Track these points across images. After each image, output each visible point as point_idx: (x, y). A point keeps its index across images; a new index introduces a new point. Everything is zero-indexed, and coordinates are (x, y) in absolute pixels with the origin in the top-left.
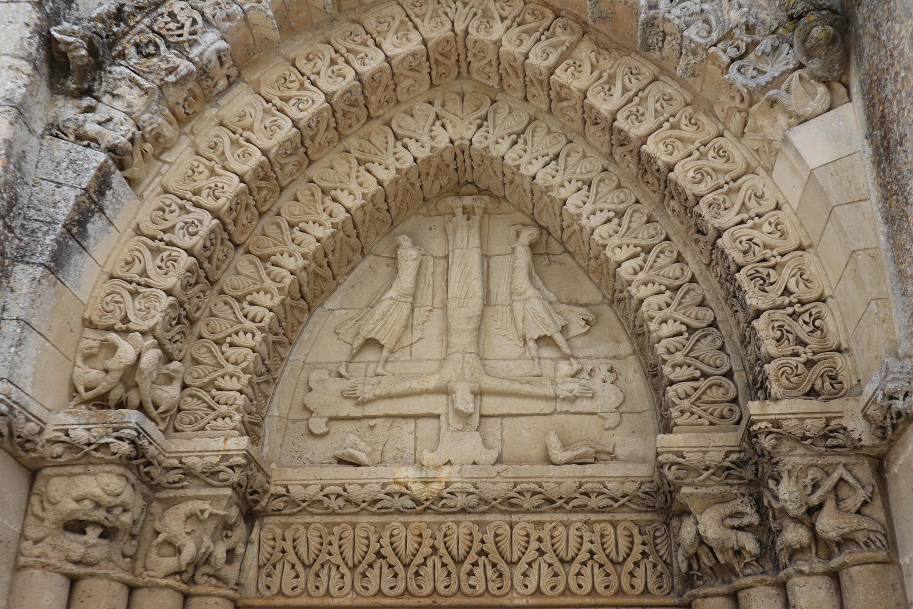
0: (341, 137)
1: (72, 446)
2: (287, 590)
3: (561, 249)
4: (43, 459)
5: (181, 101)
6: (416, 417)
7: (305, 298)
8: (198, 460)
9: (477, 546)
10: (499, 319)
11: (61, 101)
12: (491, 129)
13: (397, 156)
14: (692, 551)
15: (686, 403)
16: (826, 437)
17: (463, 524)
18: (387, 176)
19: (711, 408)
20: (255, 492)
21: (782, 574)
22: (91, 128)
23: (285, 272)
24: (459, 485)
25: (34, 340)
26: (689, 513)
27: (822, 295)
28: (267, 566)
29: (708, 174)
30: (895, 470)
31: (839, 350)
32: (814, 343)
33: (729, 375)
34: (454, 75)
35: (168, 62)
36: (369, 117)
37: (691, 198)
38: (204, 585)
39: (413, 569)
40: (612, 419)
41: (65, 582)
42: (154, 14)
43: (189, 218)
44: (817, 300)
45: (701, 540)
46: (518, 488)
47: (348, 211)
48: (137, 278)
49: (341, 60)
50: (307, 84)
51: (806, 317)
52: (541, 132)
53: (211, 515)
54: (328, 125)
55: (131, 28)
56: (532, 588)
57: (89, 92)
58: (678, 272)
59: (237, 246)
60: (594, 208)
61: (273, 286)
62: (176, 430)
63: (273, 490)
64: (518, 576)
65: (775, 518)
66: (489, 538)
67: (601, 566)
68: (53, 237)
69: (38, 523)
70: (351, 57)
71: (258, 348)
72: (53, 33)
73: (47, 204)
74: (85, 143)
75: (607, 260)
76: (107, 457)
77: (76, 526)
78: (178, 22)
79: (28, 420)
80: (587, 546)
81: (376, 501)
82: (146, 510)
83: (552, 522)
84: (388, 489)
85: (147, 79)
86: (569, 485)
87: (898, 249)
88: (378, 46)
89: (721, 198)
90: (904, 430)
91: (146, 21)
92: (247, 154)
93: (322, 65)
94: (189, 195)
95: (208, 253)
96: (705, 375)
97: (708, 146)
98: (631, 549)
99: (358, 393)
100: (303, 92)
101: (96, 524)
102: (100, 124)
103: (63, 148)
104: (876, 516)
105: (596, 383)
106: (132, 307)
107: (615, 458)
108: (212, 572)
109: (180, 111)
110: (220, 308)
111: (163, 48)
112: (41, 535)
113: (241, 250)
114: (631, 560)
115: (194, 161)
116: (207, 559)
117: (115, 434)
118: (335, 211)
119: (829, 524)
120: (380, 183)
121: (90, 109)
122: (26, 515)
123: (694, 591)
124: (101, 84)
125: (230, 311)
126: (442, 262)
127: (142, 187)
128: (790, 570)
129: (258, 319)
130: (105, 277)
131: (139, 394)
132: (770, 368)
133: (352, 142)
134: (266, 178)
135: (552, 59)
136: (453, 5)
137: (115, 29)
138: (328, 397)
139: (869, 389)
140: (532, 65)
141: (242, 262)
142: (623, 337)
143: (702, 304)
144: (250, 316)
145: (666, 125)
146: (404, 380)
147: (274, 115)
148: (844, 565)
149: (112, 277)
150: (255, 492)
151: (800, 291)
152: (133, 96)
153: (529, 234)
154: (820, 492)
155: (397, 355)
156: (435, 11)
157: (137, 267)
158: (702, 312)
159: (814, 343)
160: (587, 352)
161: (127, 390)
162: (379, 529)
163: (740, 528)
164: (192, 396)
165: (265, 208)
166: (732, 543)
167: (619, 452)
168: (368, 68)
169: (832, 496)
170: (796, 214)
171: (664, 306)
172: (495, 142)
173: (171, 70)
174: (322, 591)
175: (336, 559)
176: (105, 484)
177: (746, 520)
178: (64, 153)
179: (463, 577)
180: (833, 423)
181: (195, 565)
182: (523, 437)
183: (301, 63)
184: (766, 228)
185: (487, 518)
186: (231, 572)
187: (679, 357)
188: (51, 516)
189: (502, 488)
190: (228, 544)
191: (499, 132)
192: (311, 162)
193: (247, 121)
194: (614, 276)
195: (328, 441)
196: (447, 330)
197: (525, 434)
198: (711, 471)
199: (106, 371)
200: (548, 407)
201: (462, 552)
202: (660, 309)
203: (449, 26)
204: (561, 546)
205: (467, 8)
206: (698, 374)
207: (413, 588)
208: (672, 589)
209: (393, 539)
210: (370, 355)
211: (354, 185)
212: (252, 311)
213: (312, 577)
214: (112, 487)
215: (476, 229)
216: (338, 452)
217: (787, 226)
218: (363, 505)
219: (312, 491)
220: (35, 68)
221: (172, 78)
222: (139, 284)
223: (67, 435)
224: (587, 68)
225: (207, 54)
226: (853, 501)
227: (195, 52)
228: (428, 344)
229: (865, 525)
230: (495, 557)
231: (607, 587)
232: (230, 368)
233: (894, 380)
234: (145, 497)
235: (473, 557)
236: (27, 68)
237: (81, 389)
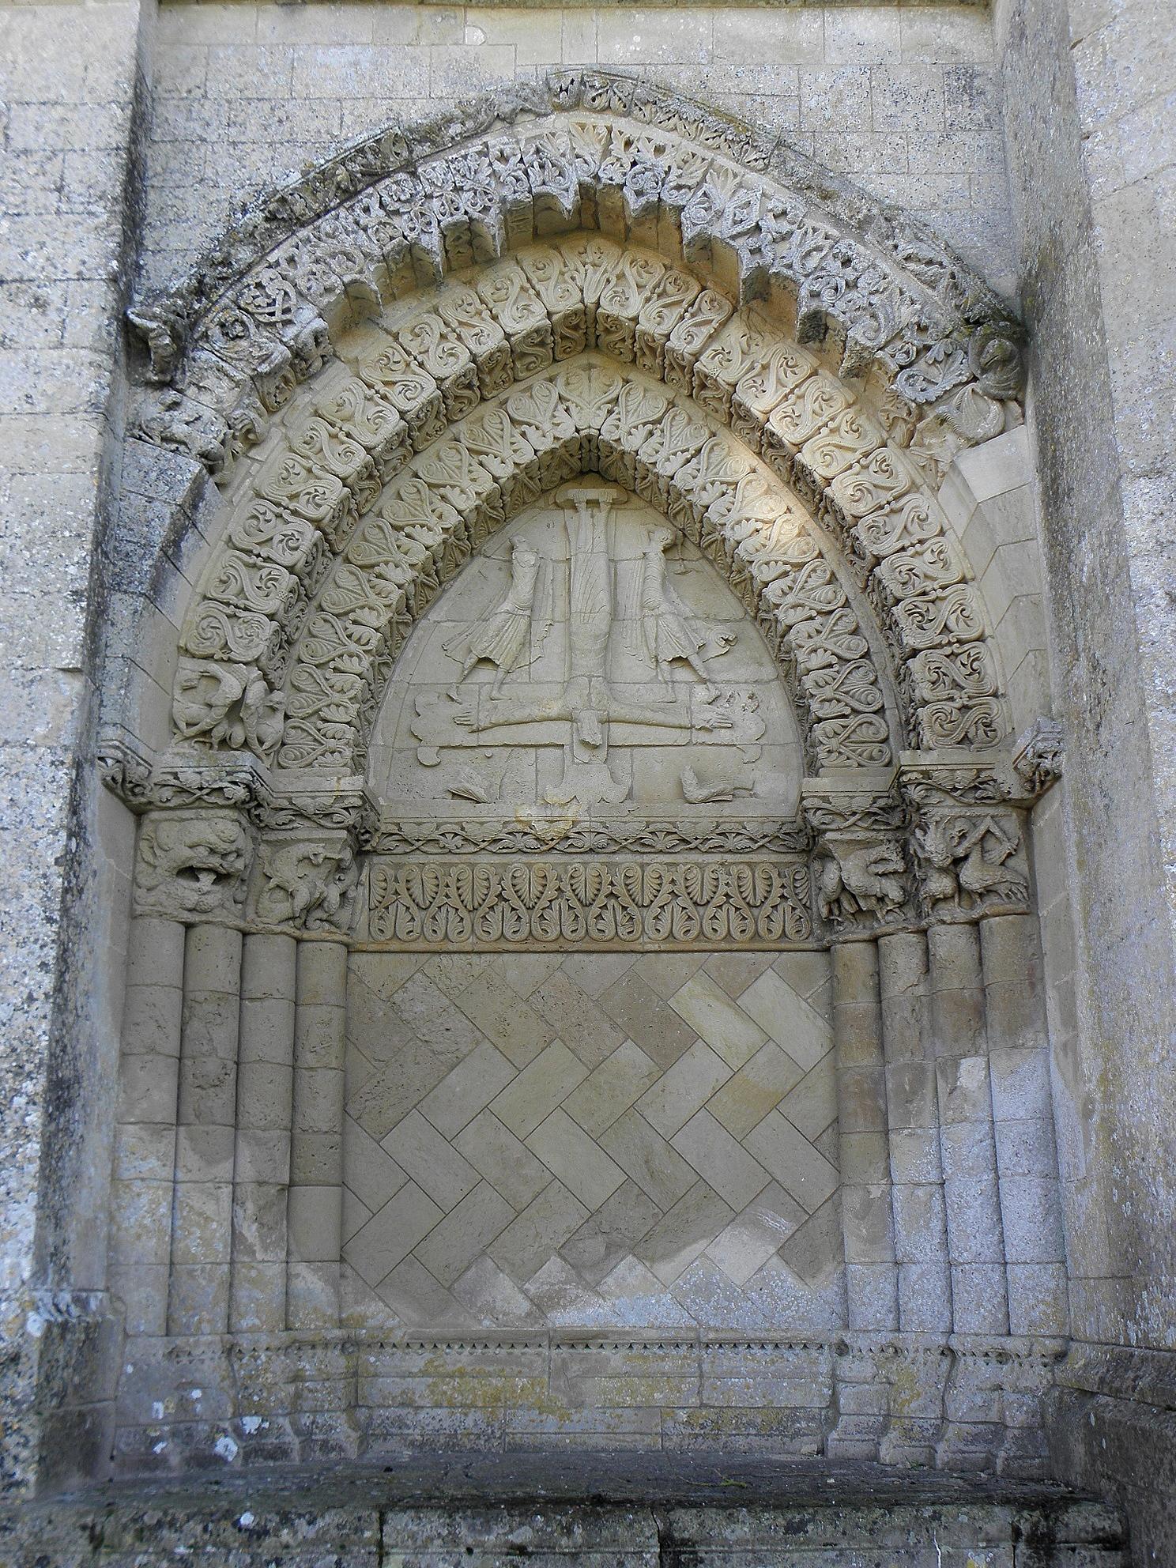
0: (450, 422)
2: (402, 935)
3: (699, 555)
4: (150, 803)
5: (273, 390)
7: (409, 613)
8: (309, 800)
9: (606, 889)
11: (141, 394)
12: (622, 416)
13: (515, 447)
14: (834, 897)
15: (834, 743)
16: (976, 788)
17: (591, 866)
18: (505, 472)
19: (860, 748)
20: (367, 832)
21: (923, 923)
22: (179, 430)
23: (392, 587)
24: (587, 824)
25: (139, 678)
26: (833, 858)
27: (982, 634)
28: (380, 908)
29: (869, 491)
30: (1041, 823)
31: (995, 695)
32: (970, 687)
34: (580, 348)
35: (261, 349)
36: (483, 399)
37: (849, 519)
38: (317, 930)
39: (537, 913)
40: (752, 752)
41: (182, 929)
42: (239, 286)
44: (977, 640)
45: (843, 887)
46: (651, 829)
47: (460, 512)
48: (234, 600)
49: (452, 337)
50: (414, 365)
51: (964, 658)
52: (682, 419)
53: (326, 858)
54: (438, 413)
55: (214, 304)
56: (664, 932)
57: (170, 384)
58: (831, 595)
59: (335, 554)
61: (379, 602)
62: (281, 767)
63: (383, 829)
64: (650, 921)
65: (919, 865)
66: (619, 880)
67: (737, 909)
68: (150, 562)
69: (151, 870)
70: (465, 332)
71: (365, 674)
72: (132, 316)
73: (139, 523)
74: (174, 446)
75: (752, 577)
76: (221, 802)
77: (190, 872)
78: (268, 297)
79: (139, 764)
80: (723, 889)
81: (495, 841)
82: (256, 856)
83: (685, 864)
84: (510, 828)
85: (235, 367)
86: (705, 826)
87: (1058, 601)
88: (495, 318)
89: (881, 520)
90: (1052, 786)
91: (230, 293)
92: (349, 453)
94: (285, 502)
95: (308, 569)
96: (855, 711)
97: (871, 457)
98: (769, 892)
99: (473, 720)
100: (411, 377)
101: (209, 870)
102: (187, 423)
103: (148, 454)
104: (1019, 869)
105: (736, 715)
106: (232, 632)
107: (755, 795)
108: (325, 916)
109: (271, 400)
110: (320, 628)
111: (253, 329)
112: (154, 883)
113: (339, 559)
114: (769, 903)
115: (289, 459)
117: (229, 778)
118: (445, 513)
119: (971, 875)
120: (496, 479)
121: (175, 405)
122: (135, 861)
123: (834, 937)
124: (184, 372)
125: (332, 631)
126: (563, 566)
127: (230, 492)
128: (932, 919)
129: (363, 641)
130: (198, 598)
131: (245, 728)
132: (923, 713)
133: (462, 428)
134: (371, 477)
135: (697, 343)
136: (582, 269)
137: (197, 306)
138: (439, 722)
139: (1021, 743)
140: (673, 350)
141: (341, 573)
142: (766, 659)
143: (855, 632)
144: (355, 637)
145: (825, 431)
146: (523, 706)
147: (378, 405)
148: (985, 916)
149: (205, 598)
150: (367, 832)
151: (960, 631)
153: (664, 535)
154: (966, 844)
155: (513, 676)
156: (562, 274)
157: (234, 587)
158: (854, 641)
159: (970, 687)
160: (725, 676)
161: (231, 726)
162: (500, 870)
163: (883, 875)
164: (294, 728)
165: (364, 511)
166: (877, 890)
167: (760, 789)
168: (484, 348)
169: (978, 848)
170: (960, 542)
171: (814, 633)
173: (264, 359)
174: (441, 935)
175: (455, 901)
176: (220, 829)
177: (891, 868)
178: (152, 461)
179: (592, 921)
180: (983, 775)
181: (308, 909)
183: (405, 338)
184: (928, 557)
185: (617, 858)
186: (343, 917)
187: (828, 692)
188: (164, 863)
190: (341, 887)
191: (633, 420)
192: (416, 453)
193: (347, 411)
194: (760, 595)
195: (439, 770)
197: (658, 767)
198: (857, 816)
199: (210, 706)
200: (681, 737)
201: (590, 895)
202: (810, 637)
203: (577, 295)
204: (696, 890)
205: (599, 274)
206: (848, 711)
207: (538, 932)
208: (811, 933)
209: (516, 881)
210: (485, 674)
211: (465, 482)
213: (428, 922)
214: (228, 833)
215: (601, 528)
216: (453, 787)
217: (950, 555)
218: (483, 845)
219: (427, 830)
220: (116, 362)
221: (264, 368)
222: (236, 607)
223: (176, 778)
224: (737, 356)
225: (303, 336)
226: (998, 851)
227: (290, 332)
228: (549, 662)
229: (1008, 878)
230: (625, 900)
231: (743, 931)
232: (336, 697)
233: (1044, 740)
234: (254, 839)
235: (601, 900)
236: (106, 361)
237: (182, 725)
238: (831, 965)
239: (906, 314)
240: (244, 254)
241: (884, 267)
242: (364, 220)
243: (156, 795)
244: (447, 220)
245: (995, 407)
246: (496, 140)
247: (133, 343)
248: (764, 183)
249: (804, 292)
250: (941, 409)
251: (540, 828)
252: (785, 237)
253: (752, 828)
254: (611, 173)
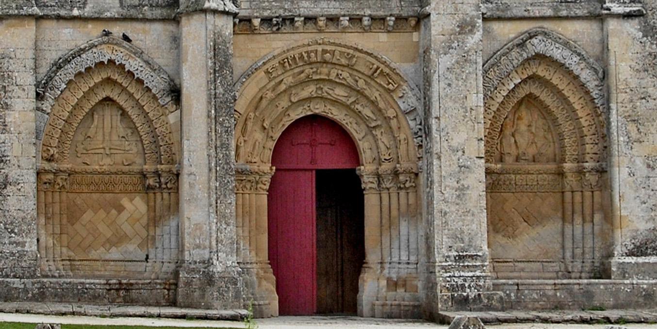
1: (45, 170)
6: (98, 153)
10: (114, 131)
18: (93, 104)
22: (44, 109)
31: (174, 154)
33: (157, 153)
43: (59, 122)
45: (149, 184)
60: (133, 113)
77: (45, 183)
86: (127, 170)
93: (82, 84)
106: (51, 141)
116: (63, 186)
121: (43, 104)
143: (153, 137)
151: (169, 142)
152: (50, 100)
159: (170, 153)
167: (137, 162)
172: (114, 95)
182: (118, 158)
187: (148, 148)
189: (115, 171)
196: (104, 135)
200: (123, 152)
210: (89, 139)
212: (69, 136)
217: (168, 128)
219: (80, 171)
238: (148, 197)
239: (162, 87)
240: (53, 75)
241: (158, 78)
242: (72, 66)
244: (86, 66)
245: (175, 106)
246: (94, 50)
248: (139, 60)
249: (145, 82)
250: (166, 106)
251: (99, 170)
252: (142, 71)
253: (135, 171)
254: (113, 57)
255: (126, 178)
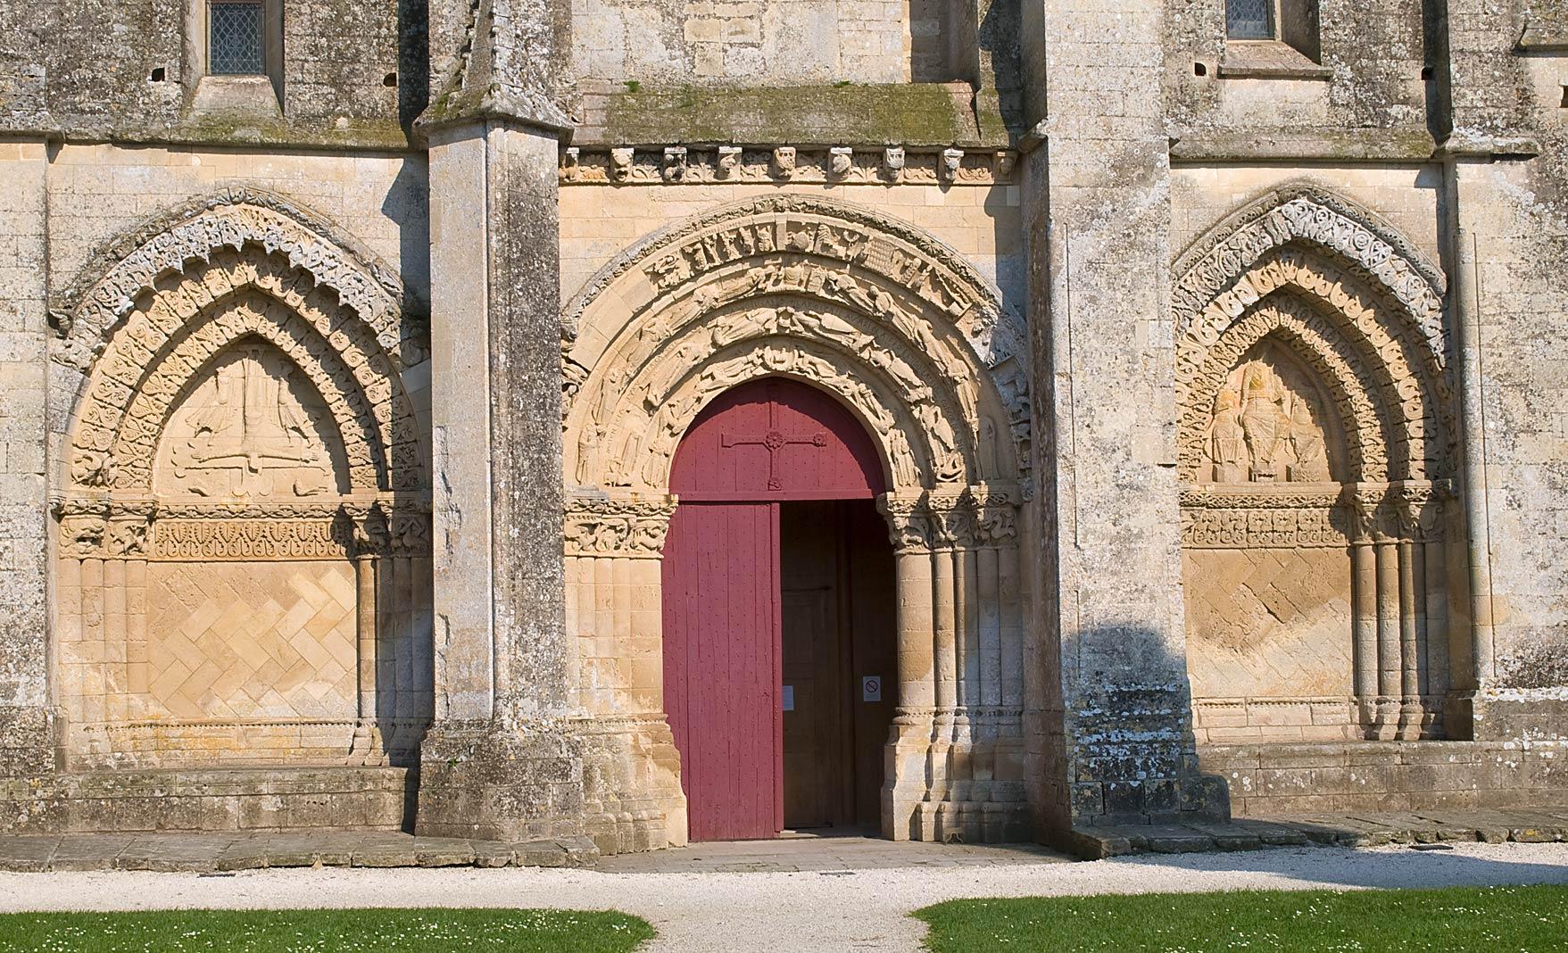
22: (73, 358)
32: (409, 462)
77: (82, 539)
119: (406, 540)
159: (409, 462)
188: (72, 536)
210: (206, 433)
227: (117, 311)
240: (96, 275)
243: (67, 509)
247: (53, 322)
251: (232, 508)
255: (304, 526)
